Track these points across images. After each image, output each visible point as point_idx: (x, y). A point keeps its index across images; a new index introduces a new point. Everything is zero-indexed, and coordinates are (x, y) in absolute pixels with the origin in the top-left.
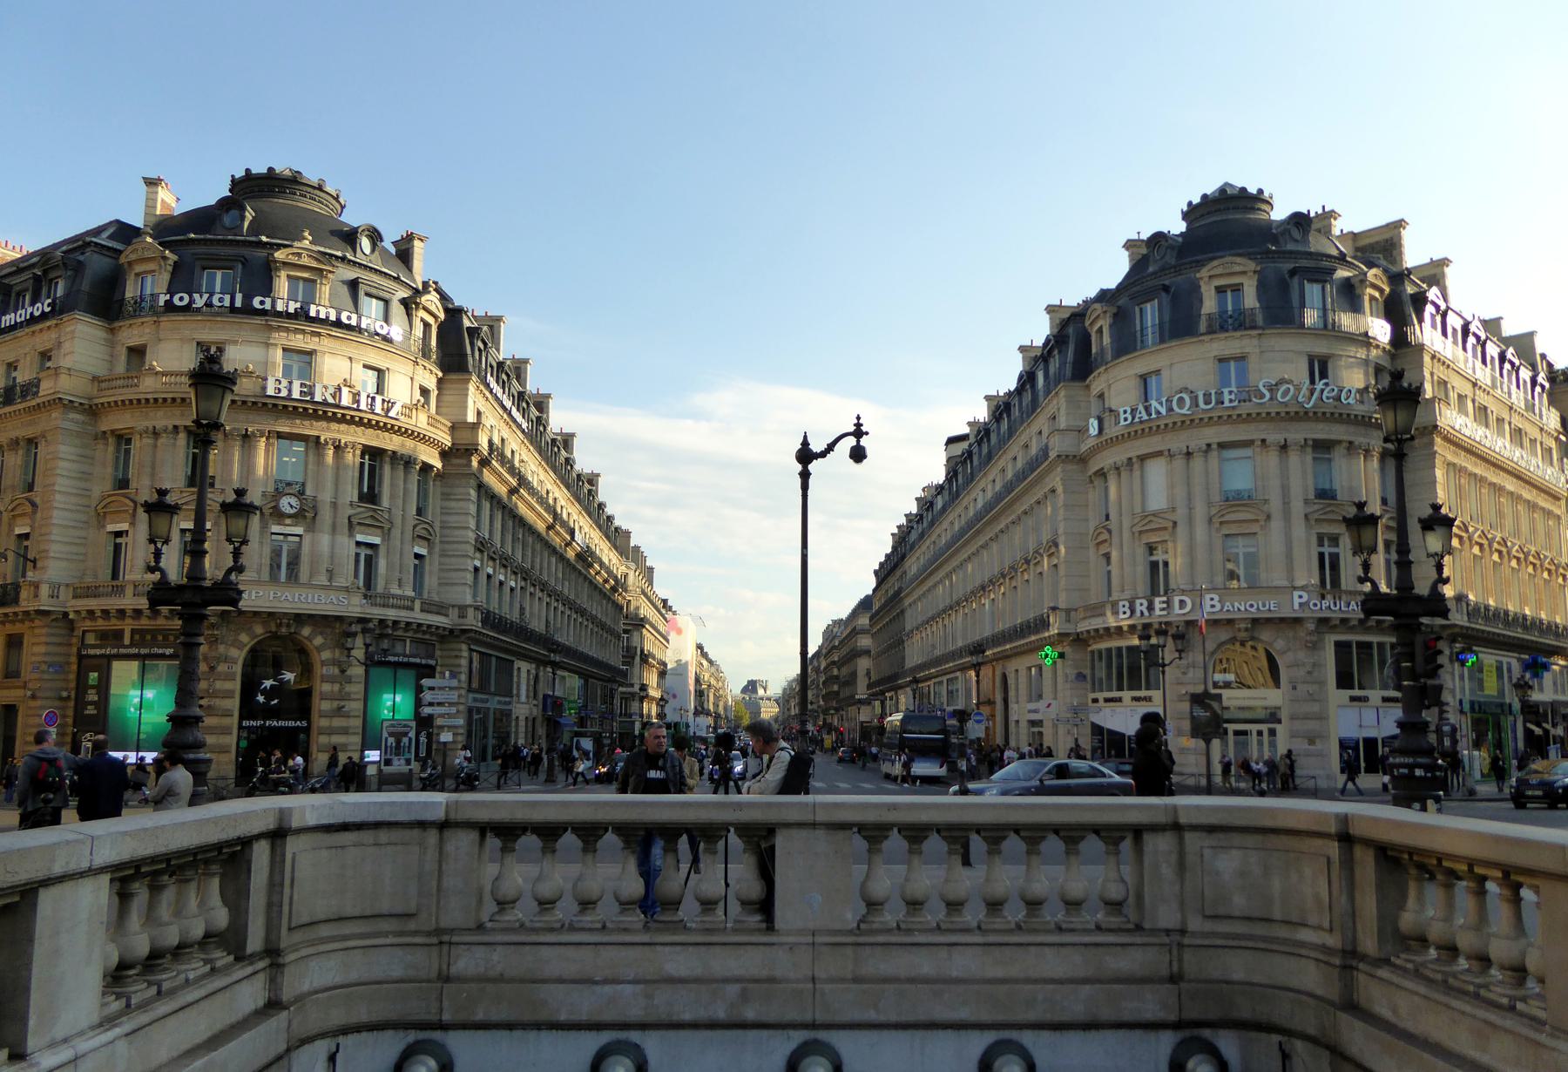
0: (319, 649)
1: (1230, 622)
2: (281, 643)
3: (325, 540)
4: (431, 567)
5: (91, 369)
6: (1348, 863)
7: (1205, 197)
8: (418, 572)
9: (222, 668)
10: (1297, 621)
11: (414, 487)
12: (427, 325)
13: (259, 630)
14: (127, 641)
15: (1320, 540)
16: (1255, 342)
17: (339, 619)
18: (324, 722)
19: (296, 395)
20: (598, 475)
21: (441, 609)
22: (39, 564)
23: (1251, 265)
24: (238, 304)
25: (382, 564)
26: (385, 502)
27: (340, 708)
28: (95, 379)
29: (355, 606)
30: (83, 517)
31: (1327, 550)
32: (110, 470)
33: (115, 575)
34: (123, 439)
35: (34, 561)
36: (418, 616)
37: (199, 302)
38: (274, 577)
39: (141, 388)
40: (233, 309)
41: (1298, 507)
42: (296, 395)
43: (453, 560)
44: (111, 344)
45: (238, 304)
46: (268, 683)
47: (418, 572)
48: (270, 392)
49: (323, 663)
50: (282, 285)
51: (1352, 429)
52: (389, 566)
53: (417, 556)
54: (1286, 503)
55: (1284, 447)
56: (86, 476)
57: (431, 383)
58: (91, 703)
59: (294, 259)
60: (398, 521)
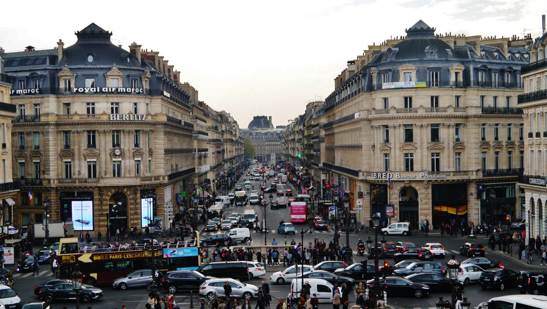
0: (129, 195)
1: (403, 181)
2: (119, 194)
3: (127, 161)
4: (153, 163)
5: (56, 113)
7: (410, 29)
9: (104, 202)
11: (147, 139)
12: (146, 81)
13: (113, 191)
14: (76, 195)
15: (433, 155)
16: (414, 92)
17: (135, 186)
18: (132, 217)
19: (118, 119)
20: (179, 72)
21: (157, 178)
22: (46, 172)
23: (414, 67)
24: (98, 91)
26: (141, 146)
27: (136, 212)
28: (57, 115)
29: (138, 182)
30: (56, 157)
31: (435, 157)
32: (62, 142)
34: (67, 132)
35: (44, 171)
36: (153, 182)
37: (87, 91)
38: (114, 175)
39: (73, 119)
40: (96, 92)
41: (425, 145)
42: (118, 119)
43: (159, 160)
44: (58, 102)
45: (98, 91)
46: (115, 206)
48: (111, 119)
49: (130, 199)
51: (444, 119)
54: (422, 144)
55: (422, 126)
56: (56, 145)
58: (66, 213)
59: (112, 74)
60: (145, 152)
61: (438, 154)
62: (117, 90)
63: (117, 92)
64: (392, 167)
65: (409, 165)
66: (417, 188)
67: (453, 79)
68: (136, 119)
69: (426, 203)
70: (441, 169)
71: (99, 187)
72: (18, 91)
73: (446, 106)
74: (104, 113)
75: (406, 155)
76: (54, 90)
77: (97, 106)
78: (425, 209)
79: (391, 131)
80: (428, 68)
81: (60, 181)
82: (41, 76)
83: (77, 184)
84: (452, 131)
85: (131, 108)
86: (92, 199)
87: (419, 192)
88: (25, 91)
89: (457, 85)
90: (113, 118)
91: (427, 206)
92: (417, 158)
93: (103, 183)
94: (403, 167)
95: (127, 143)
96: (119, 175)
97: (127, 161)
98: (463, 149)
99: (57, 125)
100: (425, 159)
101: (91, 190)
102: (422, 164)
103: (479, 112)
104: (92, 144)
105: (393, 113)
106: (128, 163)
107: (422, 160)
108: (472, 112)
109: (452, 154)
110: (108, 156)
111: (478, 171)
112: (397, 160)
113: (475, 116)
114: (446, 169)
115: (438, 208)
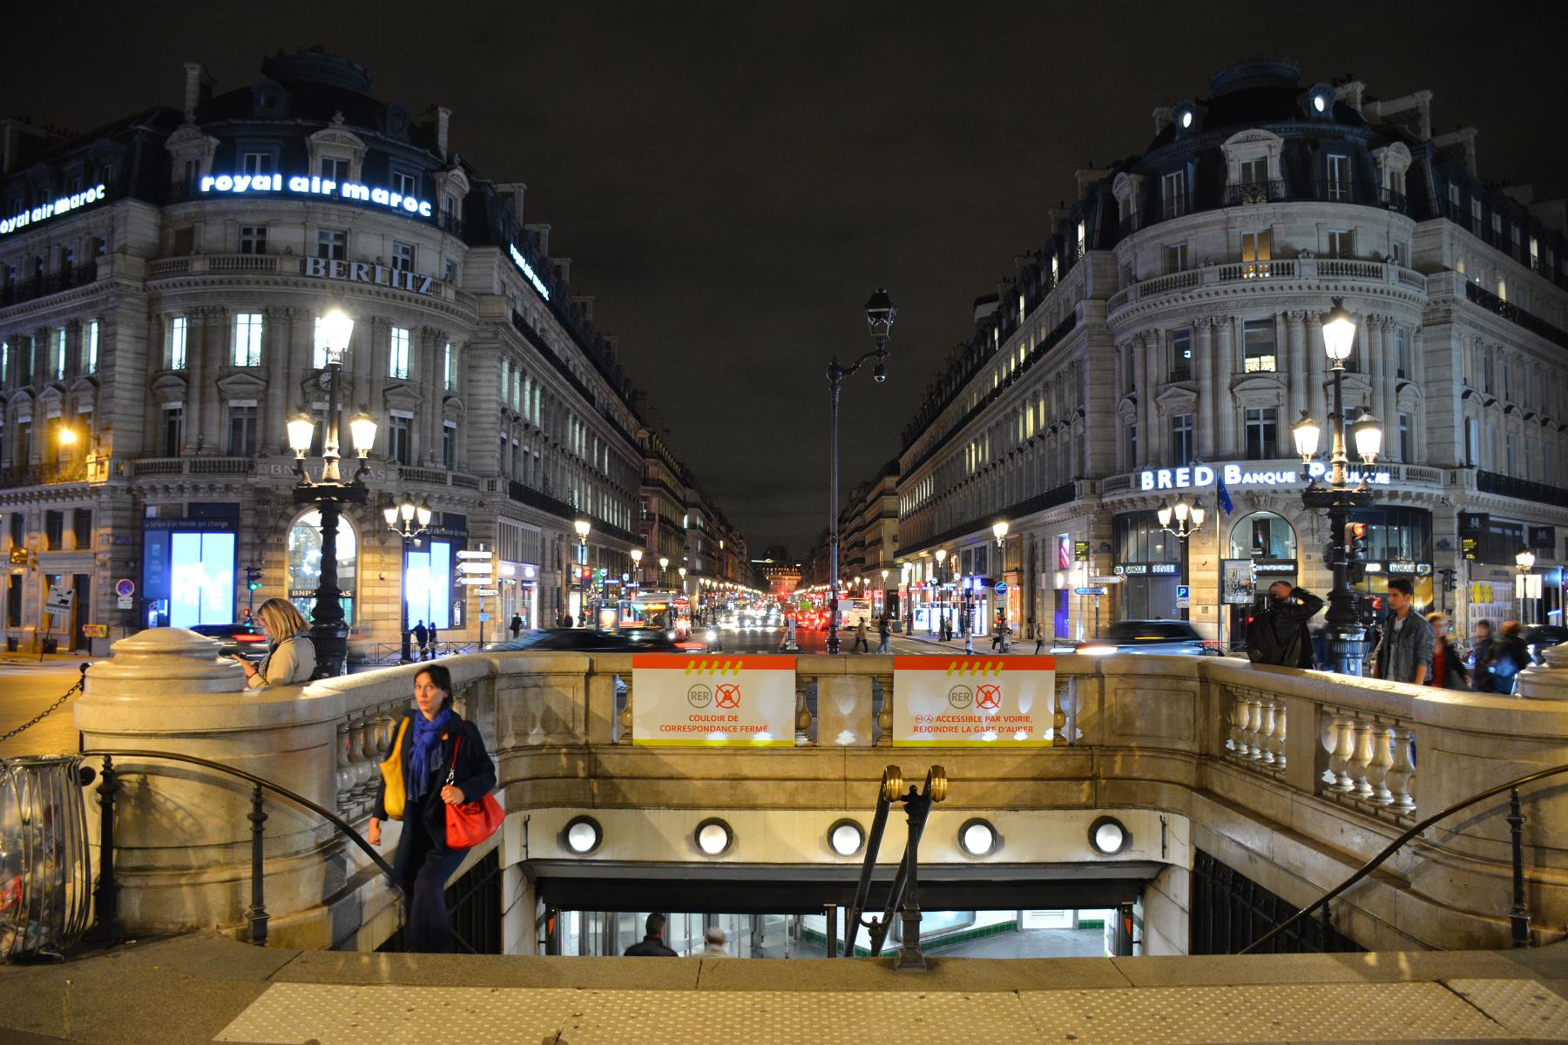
6: (1206, 696)
8: (448, 445)
25: (415, 438)
47: (448, 445)
52: (421, 440)
53: (446, 429)
57: (456, 257)
68: (395, 283)
89: (1395, 203)
90: (316, 271)
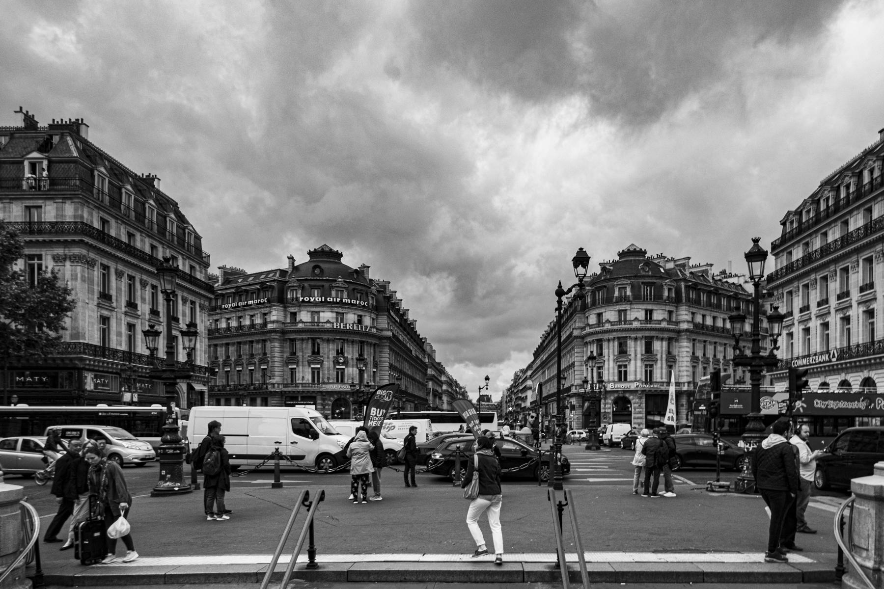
1: (617, 392)
10: (636, 391)
15: (646, 366)
28: (283, 323)
33: (292, 381)
34: (293, 341)
37: (312, 300)
38: (338, 381)
40: (321, 302)
41: (639, 356)
44: (285, 311)
50: (333, 293)
54: (636, 355)
56: (282, 352)
61: (651, 366)
62: (341, 300)
63: (341, 304)
64: (605, 378)
65: (623, 376)
66: (631, 397)
67: (666, 294)
69: (640, 413)
70: (654, 380)
71: (321, 392)
72: (250, 302)
73: (661, 318)
74: (328, 322)
75: (620, 366)
76: (282, 300)
77: (322, 314)
78: (638, 418)
79: (605, 344)
80: (643, 283)
81: (286, 386)
82: (270, 287)
83: (300, 388)
84: (665, 343)
85: (356, 318)
86: (315, 404)
87: (632, 402)
88: (256, 302)
91: (640, 415)
92: (631, 368)
93: (325, 388)
94: (616, 378)
95: (351, 353)
96: (342, 381)
97: (351, 369)
98: (675, 362)
99: (283, 332)
100: (638, 370)
101: (314, 395)
102: (636, 375)
103: (691, 326)
104: (316, 352)
105: (608, 326)
106: (352, 372)
107: (636, 371)
108: (684, 326)
109: (664, 366)
110: (331, 364)
111: (689, 383)
112: (611, 371)
113: (687, 330)
114: (659, 380)
115: (650, 418)
